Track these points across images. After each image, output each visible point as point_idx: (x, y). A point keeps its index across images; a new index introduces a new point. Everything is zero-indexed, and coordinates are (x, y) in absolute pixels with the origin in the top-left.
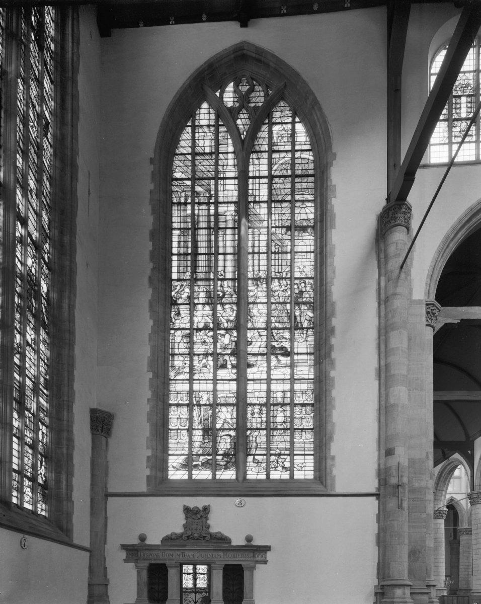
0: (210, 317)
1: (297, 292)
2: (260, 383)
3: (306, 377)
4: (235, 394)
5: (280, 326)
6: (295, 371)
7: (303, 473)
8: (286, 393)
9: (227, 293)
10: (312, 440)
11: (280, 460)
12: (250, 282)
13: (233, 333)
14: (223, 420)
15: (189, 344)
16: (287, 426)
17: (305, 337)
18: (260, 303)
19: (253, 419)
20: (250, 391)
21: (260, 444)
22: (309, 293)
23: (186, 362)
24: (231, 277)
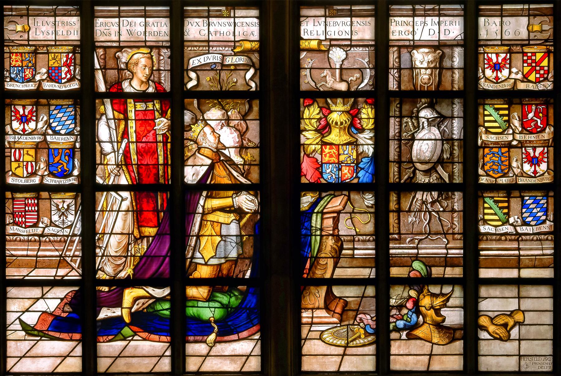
4: (256, 58)
7: (511, 347)
8: (447, 51)
11: (426, 301)
14: (207, 152)
16: (451, 176)
19: (327, 150)
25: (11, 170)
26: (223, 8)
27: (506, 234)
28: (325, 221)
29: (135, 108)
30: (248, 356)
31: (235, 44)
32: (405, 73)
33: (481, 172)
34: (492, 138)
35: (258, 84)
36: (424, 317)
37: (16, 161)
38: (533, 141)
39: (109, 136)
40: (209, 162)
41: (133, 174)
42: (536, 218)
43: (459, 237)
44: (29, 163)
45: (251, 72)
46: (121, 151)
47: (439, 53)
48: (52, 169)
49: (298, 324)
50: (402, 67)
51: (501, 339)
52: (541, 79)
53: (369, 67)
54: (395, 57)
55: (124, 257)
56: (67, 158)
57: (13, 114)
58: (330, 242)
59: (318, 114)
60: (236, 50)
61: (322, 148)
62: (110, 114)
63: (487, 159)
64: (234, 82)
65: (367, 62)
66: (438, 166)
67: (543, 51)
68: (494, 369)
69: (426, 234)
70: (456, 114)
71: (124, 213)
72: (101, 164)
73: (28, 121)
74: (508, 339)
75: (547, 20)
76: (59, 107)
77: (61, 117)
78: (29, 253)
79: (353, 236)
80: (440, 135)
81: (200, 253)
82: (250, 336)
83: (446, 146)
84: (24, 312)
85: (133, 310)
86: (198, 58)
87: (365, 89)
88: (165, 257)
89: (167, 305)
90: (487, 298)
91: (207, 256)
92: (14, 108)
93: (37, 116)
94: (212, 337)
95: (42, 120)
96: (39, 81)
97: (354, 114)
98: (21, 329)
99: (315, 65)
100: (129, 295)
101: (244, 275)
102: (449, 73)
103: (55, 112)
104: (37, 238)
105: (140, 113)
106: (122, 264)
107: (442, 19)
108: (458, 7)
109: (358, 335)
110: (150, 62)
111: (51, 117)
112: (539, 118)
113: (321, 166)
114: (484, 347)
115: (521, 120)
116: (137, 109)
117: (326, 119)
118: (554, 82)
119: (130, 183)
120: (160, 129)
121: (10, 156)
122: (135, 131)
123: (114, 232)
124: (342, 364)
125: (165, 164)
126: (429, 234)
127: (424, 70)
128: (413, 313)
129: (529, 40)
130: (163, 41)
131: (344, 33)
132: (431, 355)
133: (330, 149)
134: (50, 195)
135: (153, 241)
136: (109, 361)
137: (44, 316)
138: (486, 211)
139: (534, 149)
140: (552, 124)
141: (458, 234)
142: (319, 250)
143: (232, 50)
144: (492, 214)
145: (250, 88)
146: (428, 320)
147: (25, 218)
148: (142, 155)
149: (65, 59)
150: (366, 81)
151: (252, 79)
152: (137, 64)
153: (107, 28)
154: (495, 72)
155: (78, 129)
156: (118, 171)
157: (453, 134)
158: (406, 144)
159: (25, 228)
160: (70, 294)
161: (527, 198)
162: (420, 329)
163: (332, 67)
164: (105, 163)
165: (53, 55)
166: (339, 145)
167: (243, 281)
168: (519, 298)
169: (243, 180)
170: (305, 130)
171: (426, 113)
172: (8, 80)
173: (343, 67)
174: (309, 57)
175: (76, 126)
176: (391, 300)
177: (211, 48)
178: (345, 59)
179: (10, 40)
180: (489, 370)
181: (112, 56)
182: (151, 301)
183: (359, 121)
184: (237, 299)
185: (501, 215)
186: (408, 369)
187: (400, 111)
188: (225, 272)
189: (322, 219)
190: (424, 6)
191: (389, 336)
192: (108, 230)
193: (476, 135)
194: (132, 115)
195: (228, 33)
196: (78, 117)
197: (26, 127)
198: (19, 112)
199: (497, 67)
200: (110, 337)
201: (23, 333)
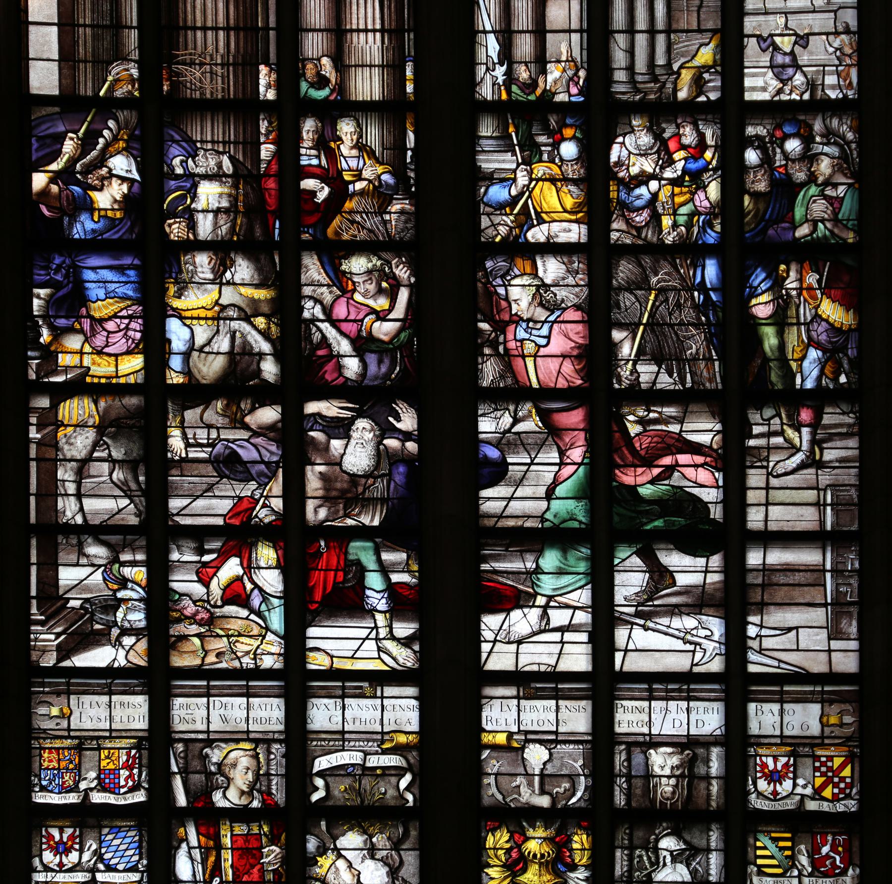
0: (260, 321)
1: (762, 186)
2: (557, 695)
3: (818, 665)
4: (413, 756)
5: (665, 381)
6: (752, 631)
8: (701, 751)
9: (359, 186)
12: (487, 128)
13: (398, 419)
15: (142, 469)
17: (805, 446)
18: (551, 248)
20: (501, 739)
22: (829, 192)
23: (127, 571)
24: (377, 96)
26: (366, 684)
29: (232, 831)
31: (383, 737)
32: (638, 783)
35: (417, 796)
47: (688, 754)
50: (633, 773)
52: (841, 796)
54: (623, 759)
57: (44, 840)
59: (507, 842)
60: (384, 747)
62: (193, 840)
64: (381, 794)
67: (844, 754)
70: (713, 845)
73: (67, 851)
75: (850, 708)
77: (119, 846)
80: (689, 877)
86: (328, 757)
87: (577, 805)
92: (47, 831)
95: (88, 850)
96: (85, 790)
97: (560, 844)
99: (503, 770)
102: (703, 785)
103: (110, 837)
105: (239, 838)
107: (692, 704)
110: (254, 762)
111: (103, 845)
112: (838, 853)
115: (810, 856)
116: (235, 833)
118: (860, 801)
120: (269, 863)
122: (232, 866)
129: (822, 737)
130: (274, 732)
140: (858, 863)
143: (378, 746)
145: (404, 802)
149: (125, 758)
150: (579, 794)
151: (408, 789)
152: (234, 765)
153: (190, 711)
154: (772, 784)
155: (145, 862)
157: (709, 874)
165: (106, 752)
170: (489, 866)
171: (668, 843)
172: (37, 789)
173: (546, 772)
174: (493, 758)
175: (141, 858)
177: (347, 743)
178: (548, 761)
179: (40, 729)
181: (197, 753)
183: (568, 854)
187: (631, 840)
194: (227, 841)
195: (373, 721)
196: (144, 844)
197: (65, 860)
198: (53, 837)
199: (774, 777)
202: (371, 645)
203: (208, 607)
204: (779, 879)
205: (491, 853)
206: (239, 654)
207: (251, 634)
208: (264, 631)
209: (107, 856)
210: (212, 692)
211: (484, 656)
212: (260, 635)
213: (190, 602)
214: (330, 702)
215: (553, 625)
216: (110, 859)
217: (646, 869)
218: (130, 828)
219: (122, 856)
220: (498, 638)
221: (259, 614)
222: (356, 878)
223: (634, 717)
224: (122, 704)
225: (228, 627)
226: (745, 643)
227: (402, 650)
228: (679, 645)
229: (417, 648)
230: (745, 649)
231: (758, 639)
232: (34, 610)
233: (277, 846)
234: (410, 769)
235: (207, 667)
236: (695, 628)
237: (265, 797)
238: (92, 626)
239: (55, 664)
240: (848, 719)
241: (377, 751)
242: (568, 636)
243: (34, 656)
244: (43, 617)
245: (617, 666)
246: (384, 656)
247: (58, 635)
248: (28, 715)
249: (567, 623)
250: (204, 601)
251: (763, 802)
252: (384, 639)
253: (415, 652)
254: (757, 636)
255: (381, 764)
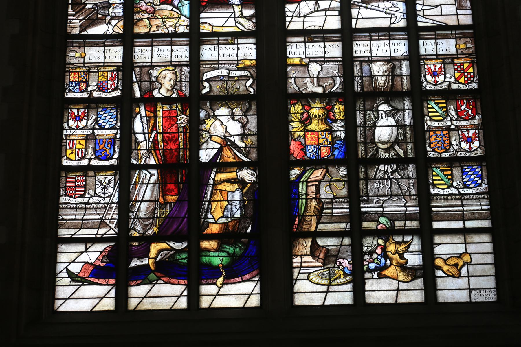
2: (324, 40)
3: (452, 22)
4: (253, 71)
7: (462, 282)
8: (397, 63)
10: (482, 189)
11: (392, 248)
14: (217, 139)
16: (406, 152)
19: (309, 135)
20: (297, 61)
21: (332, 203)
25: (66, 156)
26: (229, 38)
27: (451, 195)
28: (309, 188)
29: (162, 108)
30: (250, 295)
31: (238, 62)
32: (366, 79)
33: (428, 149)
34: (436, 124)
36: (391, 260)
37: (70, 148)
38: (467, 125)
39: (142, 129)
40: (218, 146)
41: (160, 157)
42: (474, 182)
43: (415, 197)
44: (80, 150)
45: (251, 81)
46: (151, 140)
47: (391, 65)
48: (97, 154)
49: (291, 268)
50: (364, 75)
51: (453, 276)
52: (469, 81)
53: (339, 75)
54: (358, 68)
55: (151, 218)
56: (109, 145)
57: (70, 115)
58: (314, 203)
59: (301, 110)
60: (238, 67)
61: (305, 134)
63: (432, 139)
64: (237, 89)
65: (337, 73)
66: (395, 145)
67: (469, 62)
68: (450, 301)
69: (388, 196)
70: (406, 107)
71: (152, 185)
72: (135, 149)
73: (81, 120)
74: (460, 276)
76: (104, 109)
77: (106, 117)
78: (77, 217)
79: (332, 198)
80: (395, 123)
81: (211, 214)
82: (251, 278)
83: (400, 130)
84: (70, 263)
85: (158, 260)
86: (210, 72)
87: (336, 91)
88: (184, 218)
89: (185, 256)
90: (440, 244)
91: (217, 216)
92: (71, 110)
93: (88, 116)
94: (221, 280)
95: (91, 119)
96: (91, 91)
97: (329, 110)
98: (67, 276)
99: (298, 76)
100: (154, 248)
101: (246, 230)
102: (399, 79)
104: (83, 206)
105: (166, 112)
106: (150, 224)
107: (391, 42)
108: (403, 33)
109: (338, 275)
111: (99, 117)
112: (470, 109)
113: (305, 147)
114: (441, 283)
116: (164, 109)
117: (308, 113)
119: (157, 163)
120: (181, 123)
121: (66, 145)
122: (162, 125)
123: (144, 199)
124: (326, 299)
125: (185, 149)
126: (391, 196)
127: (380, 77)
128: (382, 257)
130: (184, 62)
131: (319, 53)
132: (398, 290)
133: (311, 135)
134: (95, 173)
135: (174, 205)
136: (137, 301)
137: (86, 266)
138: (435, 178)
139: (468, 131)
140: (480, 113)
141: (414, 195)
142: (306, 210)
143: (236, 66)
144: (439, 180)
145: (249, 92)
146: (394, 262)
147: (75, 191)
148: (167, 143)
149: (110, 75)
150: (337, 86)
151: (250, 86)
152: (164, 78)
153: (143, 53)
154: (434, 77)
155: (119, 124)
156: (148, 154)
157: (405, 122)
158: (369, 130)
159: (75, 198)
160: (108, 248)
161: (465, 167)
162: (388, 270)
163: (311, 76)
164: (139, 148)
165: (102, 73)
166: (318, 132)
167: (246, 235)
168: (466, 243)
169: (245, 159)
171: (384, 107)
172: (67, 91)
174: (293, 70)
175: (117, 123)
176: (364, 247)
177: (220, 65)
179: (70, 63)
180: (446, 301)
181: (146, 72)
182: (172, 253)
183: (333, 114)
184: (240, 249)
185: (446, 180)
186: (380, 302)
187: (364, 106)
188: (231, 229)
189: (307, 187)
190: (378, 33)
191: (364, 276)
192: (140, 198)
193: (423, 122)
194: (160, 114)
195: (233, 55)
196: (119, 116)
197: (79, 124)
198: (74, 113)
199: (435, 74)
200: (139, 282)
201: (69, 280)
202: (232, 20)
203: (153, 6)
204: (441, 122)
205: (293, 115)
206: (167, 26)
207: (173, 17)
208: (180, 15)
209: (100, 122)
210: (154, 44)
211: (287, 23)
212: (178, 18)
213: (145, 4)
214: (212, 47)
215: (320, 9)
216: (102, 123)
217: (373, 120)
218: (112, 108)
219: (108, 122)
220: (294, 15)
221: (177, 8)
222: (225, 129)
223: (364, 49)
224: (110, 51)
225: (163, 14)
226: (416, 13)
227: (247, 22)
228: (383, 15)
229: (254, 20)
230: (416, 16)
231: (422, 11)
232: (70, 9)
233: (185, 115)
234: (252, 76)
235: (152, 33)
236: (391, 7)
237: (179, 92)
238: (97, 16)
239: (78, 34)
240: (469, 46)
241: (235, 69)
242: (328, 13)
243: (69, 30)
244: (74, 13)
245: (353, 26)
246: (237, 25)
247: (81, 20)
248: (65, 57)
249: (328, 7)
250: (151, 3)
251: (430, 86)
252: (238, 17)
253: (253, 23)
254: (421, 9)
255: (237, 75)
